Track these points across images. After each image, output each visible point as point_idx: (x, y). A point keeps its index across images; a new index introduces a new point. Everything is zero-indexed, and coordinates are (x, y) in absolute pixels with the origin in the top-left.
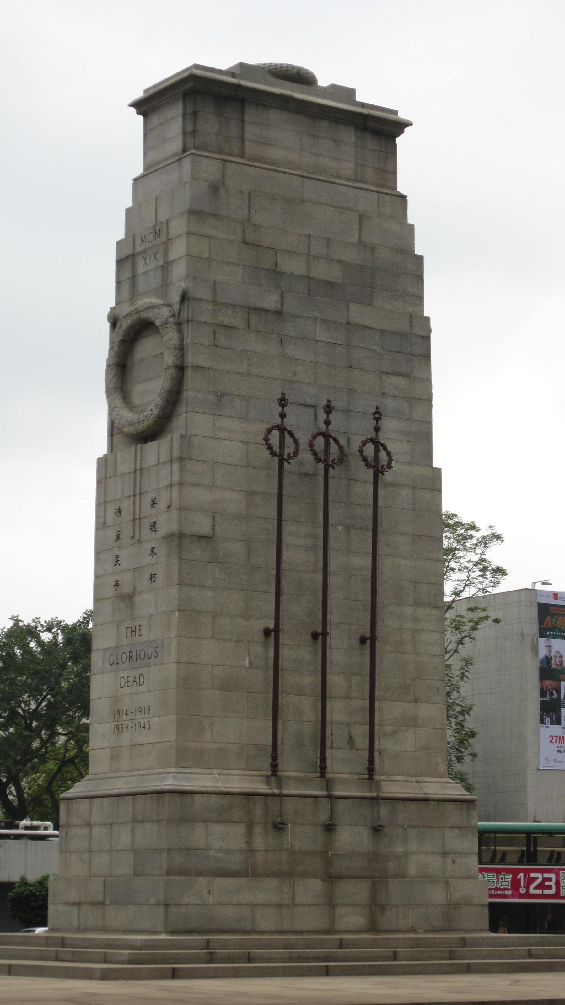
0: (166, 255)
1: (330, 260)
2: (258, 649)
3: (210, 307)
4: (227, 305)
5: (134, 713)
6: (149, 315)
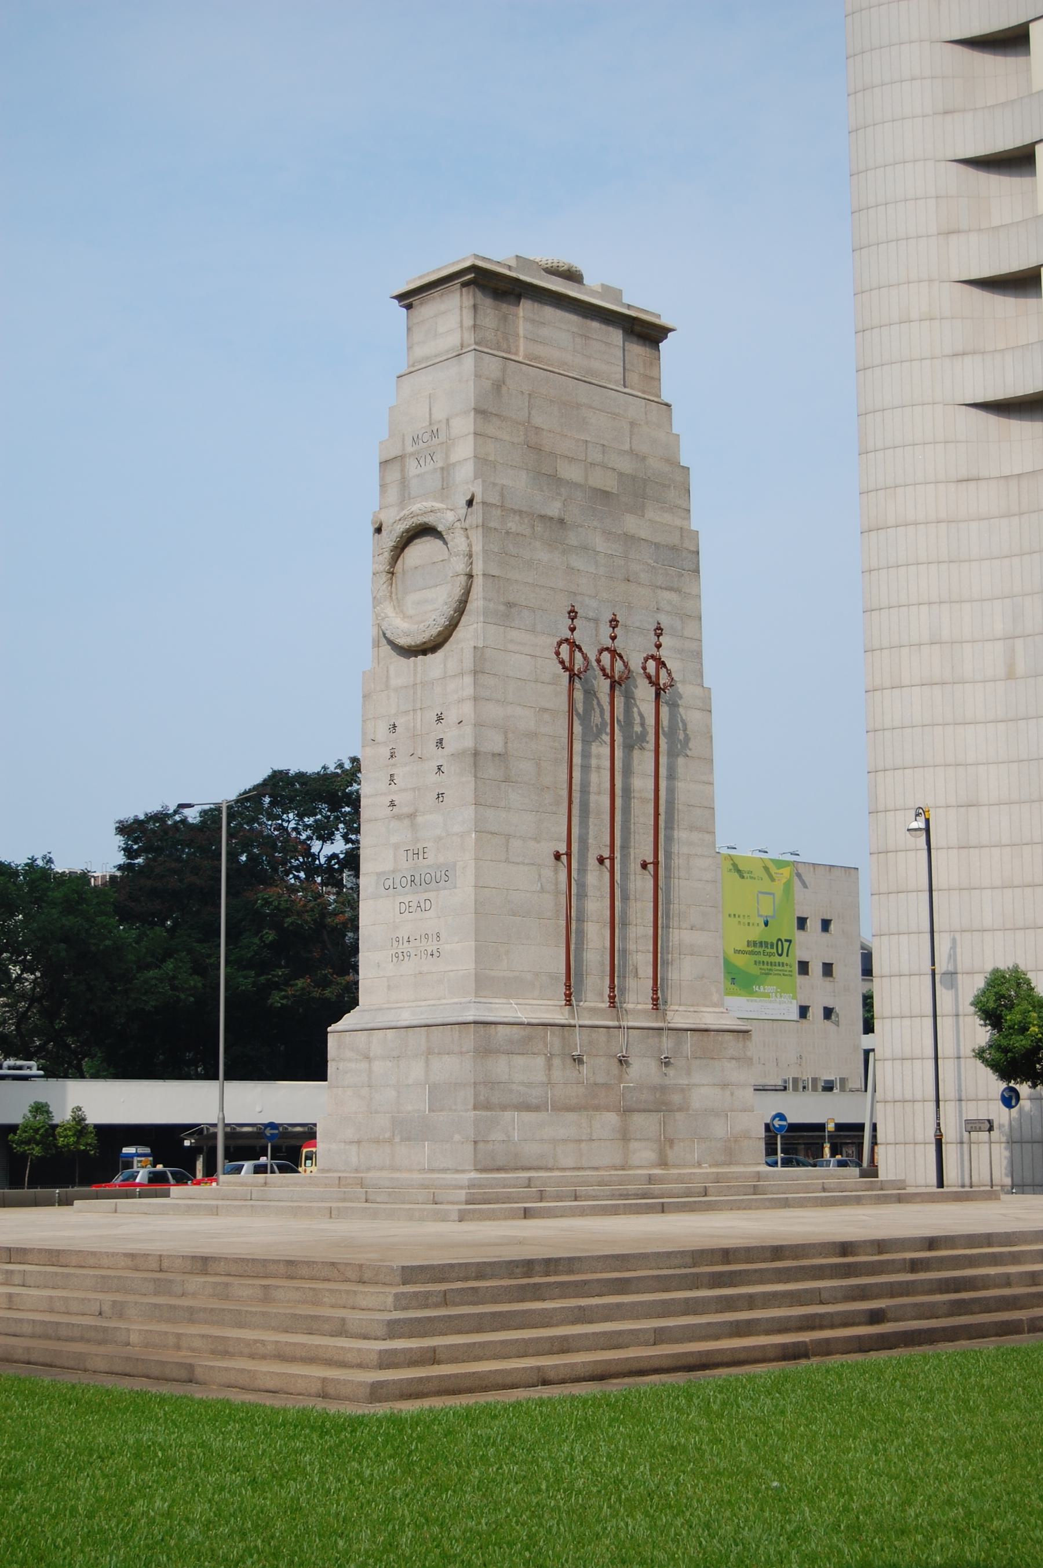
0: (447, 456)
1: (604, 467)
2: (548, 873)
3: (499, 512)
5: (419, 940)
6: (430, 519)
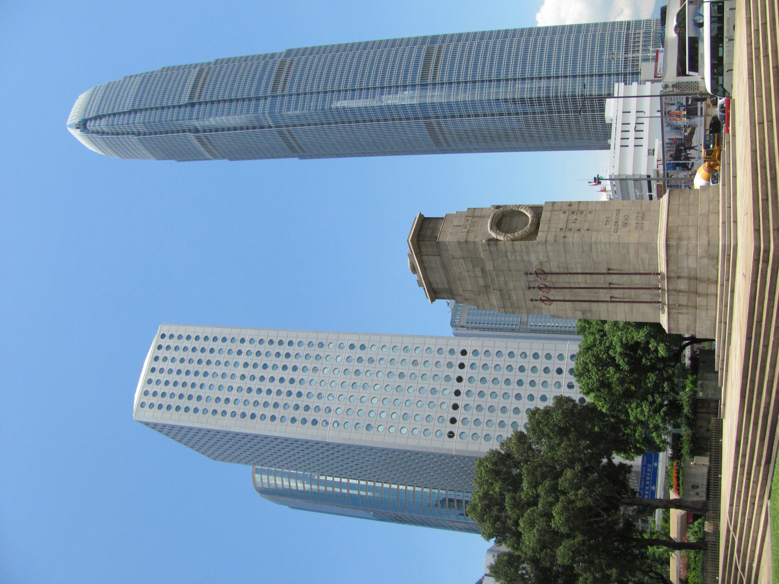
1: (474, 271)
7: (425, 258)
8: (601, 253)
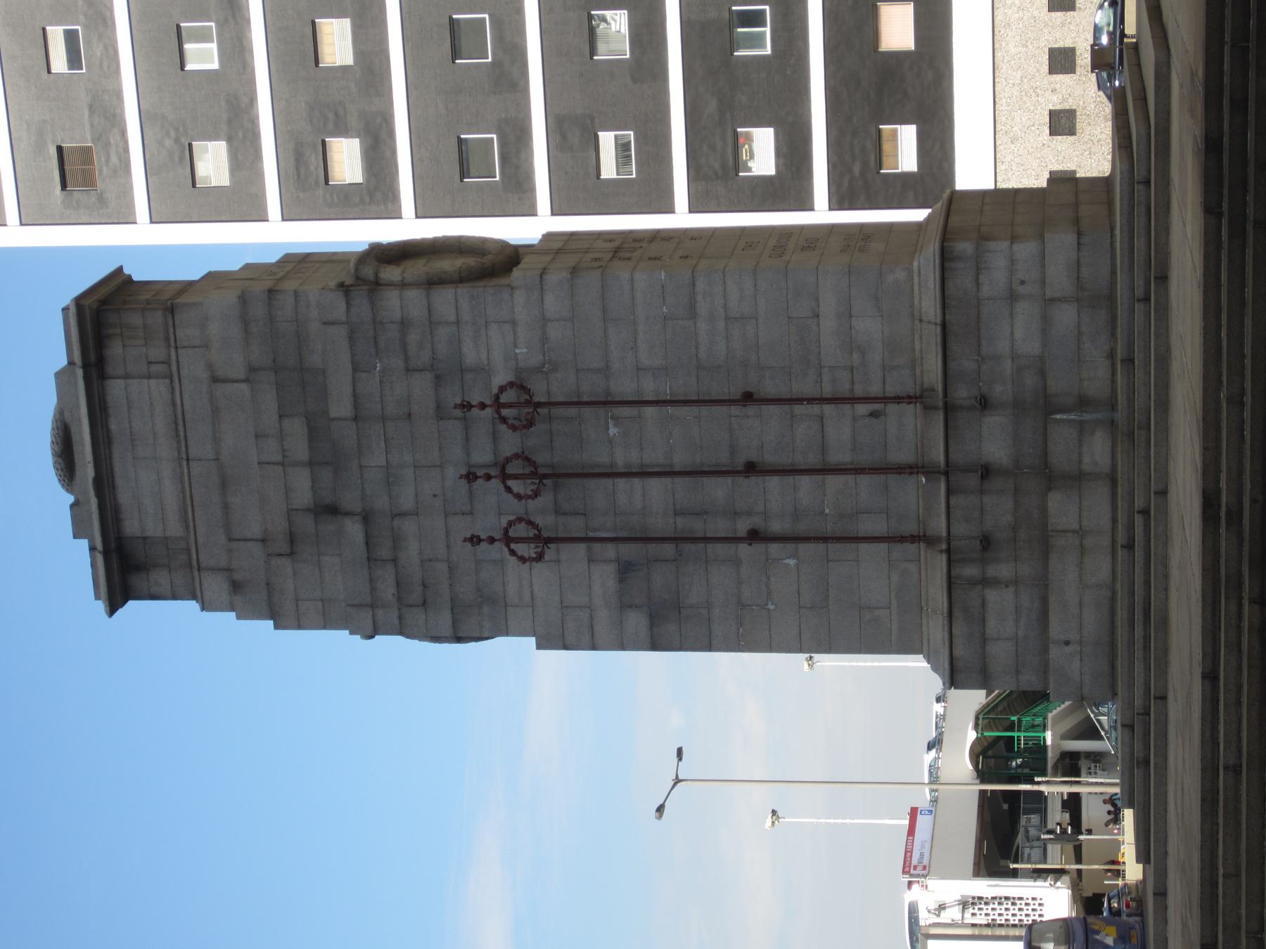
1: (281, 436)
4: (373, 590)
7: (116, 389)
8: (727, 318)
